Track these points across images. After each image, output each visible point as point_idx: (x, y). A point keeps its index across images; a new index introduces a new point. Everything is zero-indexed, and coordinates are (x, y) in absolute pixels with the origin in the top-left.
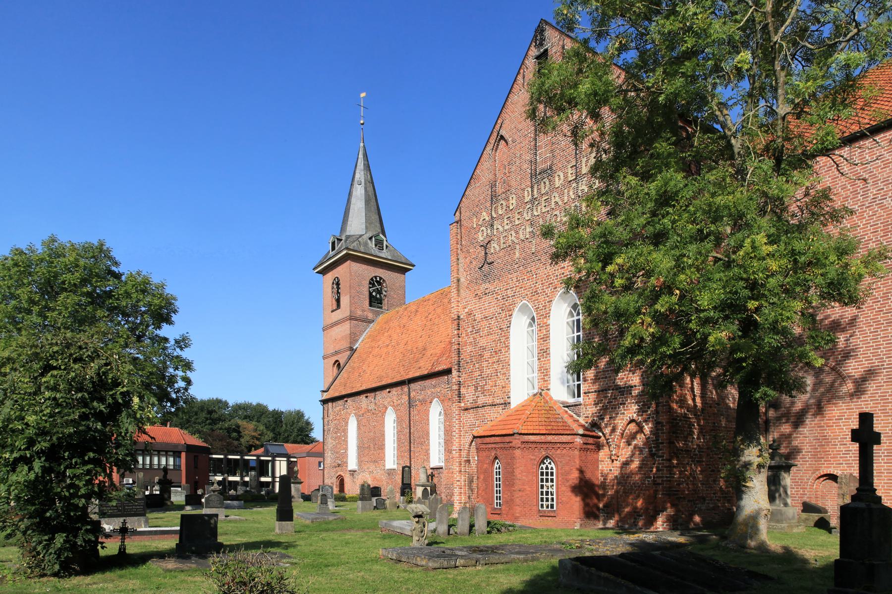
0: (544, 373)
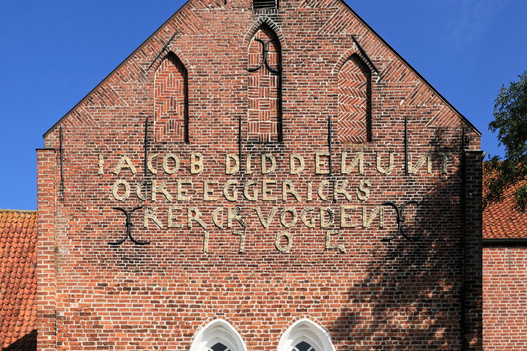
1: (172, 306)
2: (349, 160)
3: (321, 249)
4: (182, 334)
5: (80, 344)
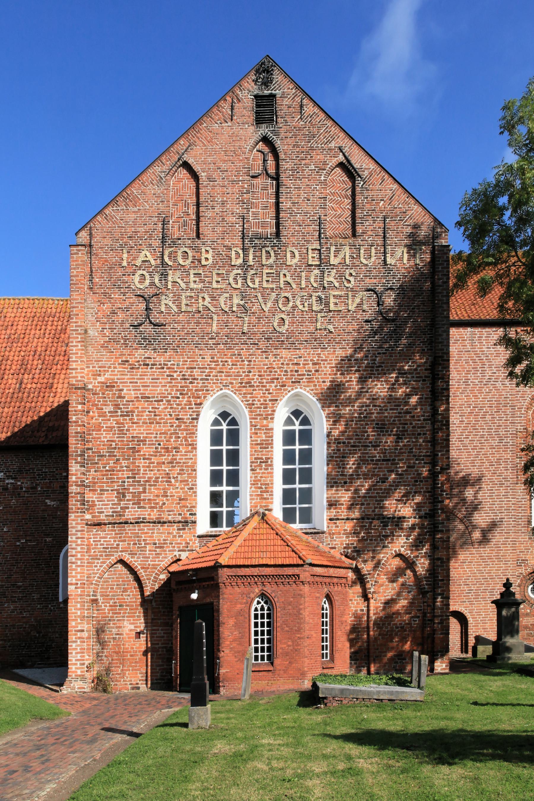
1: (185, 379)
2: (337, 252)
3: (312, 329)
4: (193, 403)
5: (105, 412)
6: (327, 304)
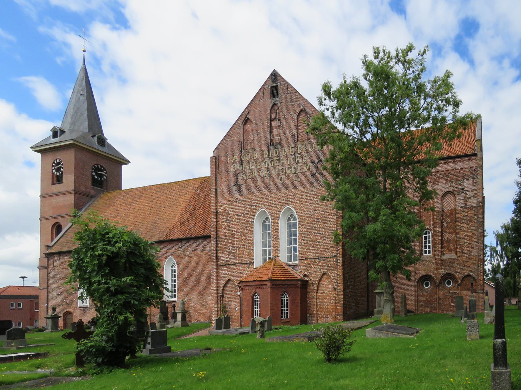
0: (276, 248)
2: (300, 148)
3: (292, 181)
6: (297, 170)
